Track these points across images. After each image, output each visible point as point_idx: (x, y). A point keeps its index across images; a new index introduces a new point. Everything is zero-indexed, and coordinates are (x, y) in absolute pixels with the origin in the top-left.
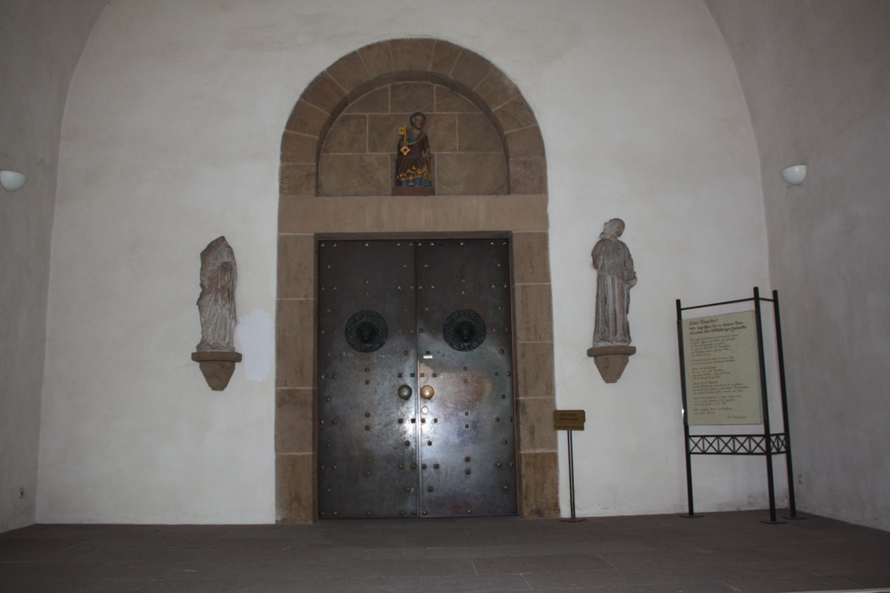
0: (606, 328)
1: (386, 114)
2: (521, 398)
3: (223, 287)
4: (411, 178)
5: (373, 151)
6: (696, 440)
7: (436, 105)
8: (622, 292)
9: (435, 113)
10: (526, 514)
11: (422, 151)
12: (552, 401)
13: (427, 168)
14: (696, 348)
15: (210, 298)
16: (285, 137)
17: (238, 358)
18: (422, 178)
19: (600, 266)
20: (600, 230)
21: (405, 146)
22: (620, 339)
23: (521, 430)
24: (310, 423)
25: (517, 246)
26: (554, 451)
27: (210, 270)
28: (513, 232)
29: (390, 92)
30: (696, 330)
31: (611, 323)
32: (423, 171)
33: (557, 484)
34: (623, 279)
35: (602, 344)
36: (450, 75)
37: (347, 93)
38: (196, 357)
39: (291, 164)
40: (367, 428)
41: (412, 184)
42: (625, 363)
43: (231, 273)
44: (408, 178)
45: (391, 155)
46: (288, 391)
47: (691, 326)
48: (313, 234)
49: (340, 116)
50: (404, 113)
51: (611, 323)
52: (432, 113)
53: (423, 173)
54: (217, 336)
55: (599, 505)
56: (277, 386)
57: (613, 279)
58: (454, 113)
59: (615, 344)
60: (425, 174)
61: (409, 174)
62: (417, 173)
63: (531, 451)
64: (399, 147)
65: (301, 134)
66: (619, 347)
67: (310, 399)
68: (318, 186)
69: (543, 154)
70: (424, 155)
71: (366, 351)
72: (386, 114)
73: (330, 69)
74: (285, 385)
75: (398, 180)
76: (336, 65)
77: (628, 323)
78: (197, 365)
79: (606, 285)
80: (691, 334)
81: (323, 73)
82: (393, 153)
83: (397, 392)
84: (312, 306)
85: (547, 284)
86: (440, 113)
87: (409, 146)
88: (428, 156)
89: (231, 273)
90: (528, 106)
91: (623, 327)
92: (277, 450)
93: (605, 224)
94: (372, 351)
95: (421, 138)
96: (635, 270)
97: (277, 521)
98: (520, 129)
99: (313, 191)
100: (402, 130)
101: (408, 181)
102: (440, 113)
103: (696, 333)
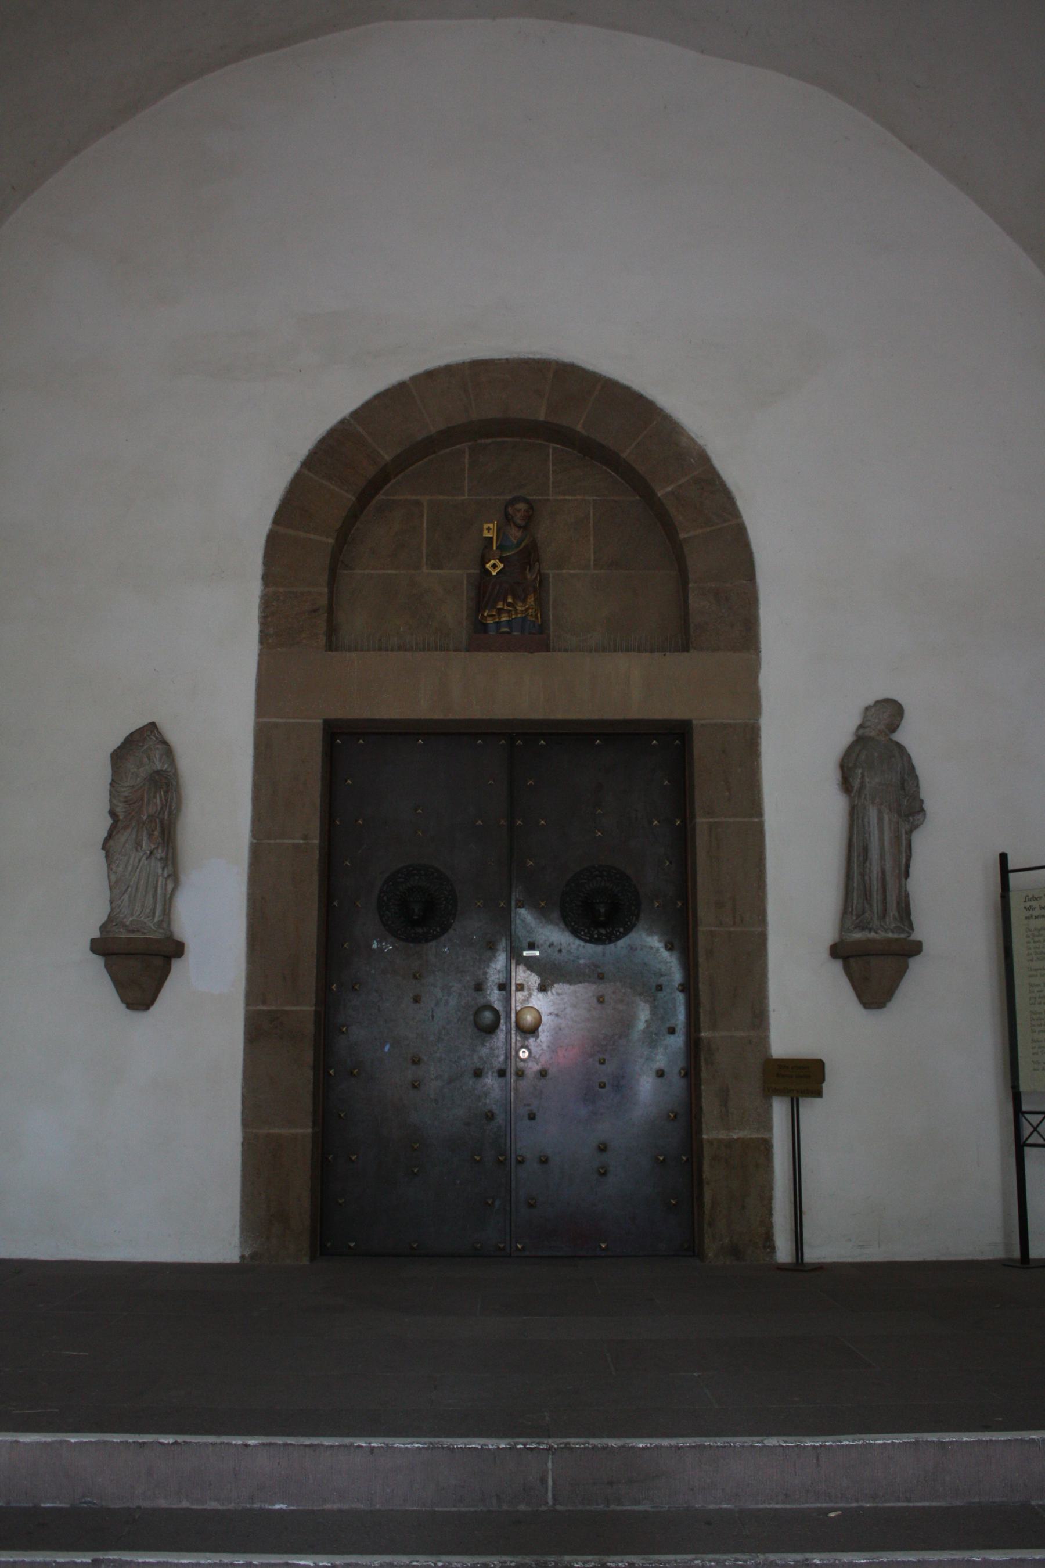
0: (867, 906)
1: (462, 498)
2: (703, 1034)
3: (151, 817)
4: (504, 618)
5: (433, 567)
6: (1035, 1119)
7: (553, 483)
8: (898, 838)
10: (711, 1255)
11: (526, 569)
12: (764, 1041)
13: (535, 601)
14: (1037, 945)
15: (123, 838)
16: (273, 542)
17: (178, 949)
18: (524, 619)
19: (856, 784)
20: (857, 721)
21: (494, 559)
22: (893, 925)
23: (704, 1094)
24: (310, 1074)
25: (700, 746)
26: (766, 1136)
27: (128, 784)
28: (694, 722)
29: (467, 456)
30: (1037, 912)
31: (876, 896)
32: (527, 606)
33: (770, 1199)
34: (900, 815)
35: (858, 935)
36: (579, 428)
37: (388, 458)
38: (98, 947)
39: (281, 590)
40: (415, 1086)
41: (504, 630)
42: (901, 972)
43: (166, 792)
44: (500, 619)
45: (469, 575)
46: (269, 1011)
47: (1028, 904)
48: (320, 721)
49: (374, 501)
50: (493, 498)
51: (876, 896)
52: (546, 498)
53: (527, 610)
54: (138, 909)
55: (850, 1240)
56: (248, 1004)
57: (880, 812)
58: (587, 498)
59: (882, 935)
60: (530, 611)
61: (500, 611)
62: (516, 610)
63: (723, 1135)
64: (484, 561)
65: (302, 534)
66: (889, 941)
67: (310, 1028)
68: (332, 630)
69: (751, 576)
70: (529, 576)
71: (417, 940)
72: (462, 498)
73: (355, 414)
74: (264, 1002)
75: (480, 621)
76: (367, 406)
77: (907, 896)
78: (98, 963)
79: (866, 824)
80: (1027, 918)
81: (343, 422)
82: (472, 571)
83: (471, 1018)
84: (317, 856)
85: (756, 820)
87: (501, 562)
88: (536, 577)
89: (166, 792)
90: (725, 485)
91: (898, 904)
92: (245, 1123)
93: (867, 709)
94: (427, 941)
95: (523, 545)
96: (922, 796)
97: (242, 1257)
98: (708, 529)
99: (323, 640)
100: (489, 529)
101: (498, 624)
103: (1036, 917)
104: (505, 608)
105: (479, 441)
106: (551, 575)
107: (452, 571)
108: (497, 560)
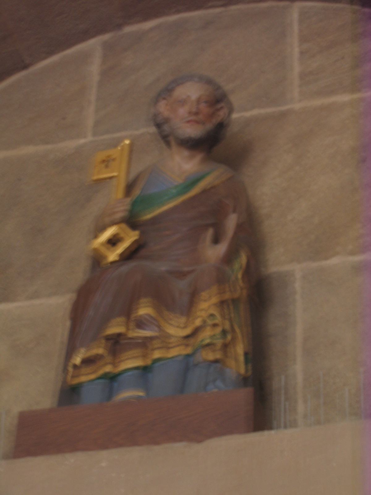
7: (303, 76)
9: (297, 106)
13: (222, 303)
44: (114, 364)
53: (196, 332)
72: (82, 141)
86: (318, 102)
102: (318, 102)
104: (131, 334)
105: (128, 29)
106: (298, 275)
107: (37, 302)
108: (124, 226)
